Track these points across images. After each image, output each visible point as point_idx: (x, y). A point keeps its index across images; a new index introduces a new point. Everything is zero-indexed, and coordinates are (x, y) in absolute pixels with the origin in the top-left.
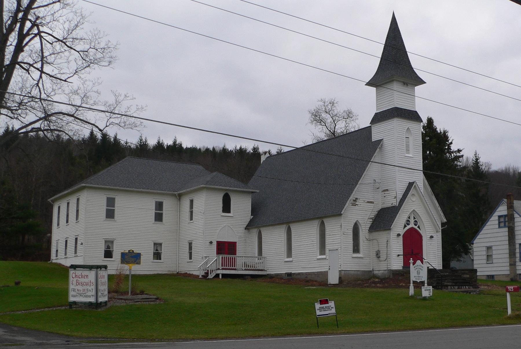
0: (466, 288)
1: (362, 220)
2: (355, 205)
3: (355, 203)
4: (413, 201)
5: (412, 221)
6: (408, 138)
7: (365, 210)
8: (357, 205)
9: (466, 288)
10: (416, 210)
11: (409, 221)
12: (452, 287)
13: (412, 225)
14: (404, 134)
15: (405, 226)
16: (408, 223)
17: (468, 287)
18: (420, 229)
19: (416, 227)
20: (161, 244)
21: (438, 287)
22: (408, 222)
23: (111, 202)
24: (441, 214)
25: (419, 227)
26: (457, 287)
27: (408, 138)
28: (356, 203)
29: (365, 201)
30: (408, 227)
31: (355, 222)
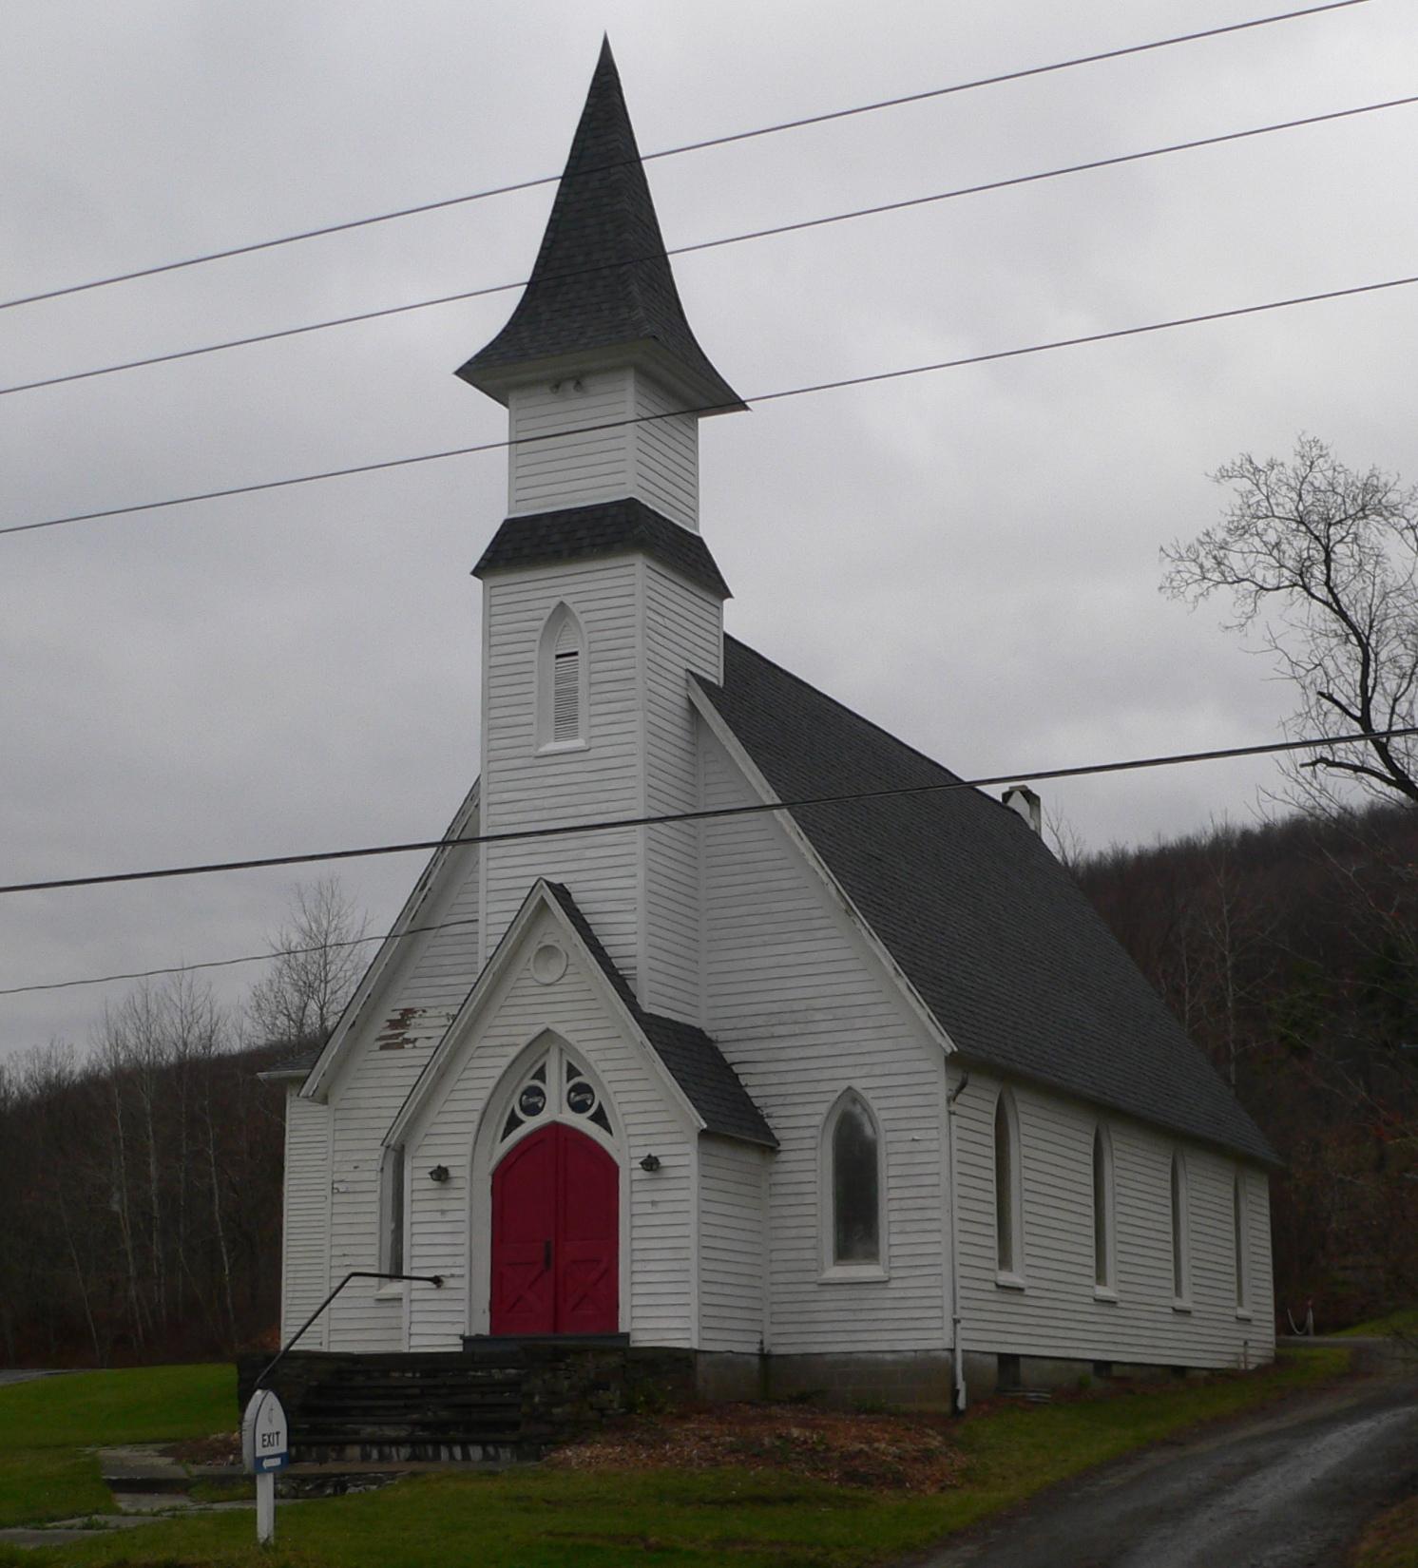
0: (466, 1456)
2: (400, 1046)
3: (403, 1034)
5: (556, 1088)
6: (575, 654)
8: (407, 1041)
9: (466, 1456)
10: (560, 1029)
11: (540, 1093)
12: (375, 1454)
13: (556, 1110)
15: (514, 1123)
16: (535, 1105)
17: (484, 1450)
18: (608, 1129)
19: (582, 1122)
22: (535, 1099)
25: (600, 1118)
26: (405, 1452)
27: (575, 654)
28: (406, 1036)
30: (531, 1124)
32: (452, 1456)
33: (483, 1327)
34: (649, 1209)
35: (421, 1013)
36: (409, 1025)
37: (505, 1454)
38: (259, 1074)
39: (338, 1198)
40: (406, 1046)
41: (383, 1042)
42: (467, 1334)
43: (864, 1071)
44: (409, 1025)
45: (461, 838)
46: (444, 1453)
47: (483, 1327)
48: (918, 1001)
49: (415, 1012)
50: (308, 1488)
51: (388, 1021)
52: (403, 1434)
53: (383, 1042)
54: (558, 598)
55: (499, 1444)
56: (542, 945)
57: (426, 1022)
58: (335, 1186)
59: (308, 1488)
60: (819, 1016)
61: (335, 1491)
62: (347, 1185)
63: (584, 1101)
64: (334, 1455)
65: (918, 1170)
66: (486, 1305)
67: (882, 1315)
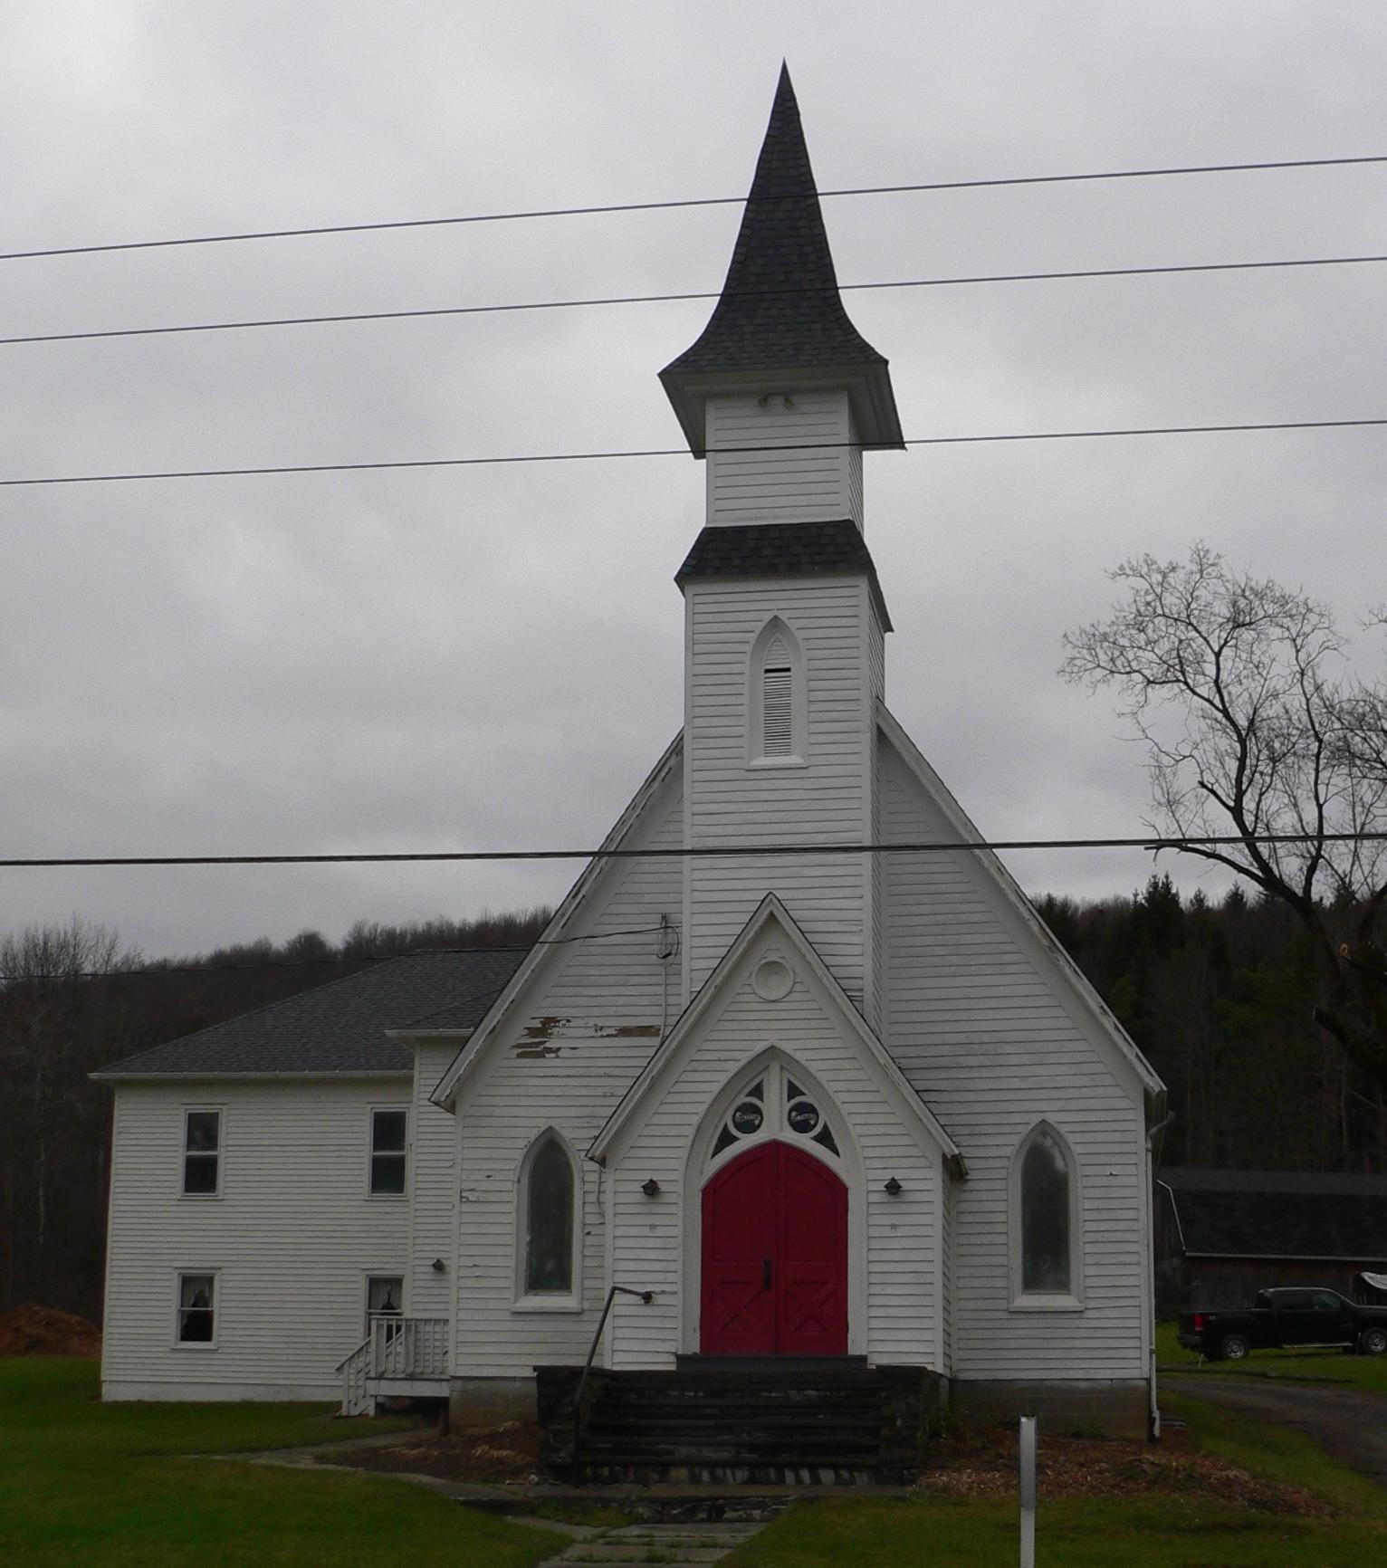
0: (816, 1480)
1: (577, 1123)
2: (541, 1055)
3: (545, 1042)
4: (774, 1001)
5: (775, 1107)
6: (788, 670)
7: (601, 1072)
8: (549, 1050)
9: (816, 1480)
10: (787, 1047)
11: (758, 1111)
12: (706, 1476)
13: (775, 1127)
14: (747, 658)
15: (726, 1139)
16: (752, 1122)
17: (837, 1475)
19: (805, 1142)
20: (396, 1282)
21: (589, 1471)
23: (203, 1131)
24: (1125, 1049)
25: (825, 1138)
26: (741, 1474)
27: (788, 670)
28: (547, 1045)
29: (601, 1029)
30: (746, 1142)
31: (533, 1134)
32: (799, 1481)
33: (694, 1347)
34: (887, 1232)
35: (564, 1022)
36: (550, 1034)
37: (862, 1478)
38: (89, 1074)
39: (466, 1208)
40: (547, 1055)
41: (520, 1050)
42: (679, 1353)
43: (1059, 1105)
44: (550, 1034)
45: (618, 850)
46: (789, 1476)
47: (694, 1347)
48: (1126, 1040)
49: (558, 1021)
50: (675, 1512)
51: (527, 1028)
52: (726, 1455)
53: (520, 1050)
54: (770, 612)
55: (851, 1468)
56: (763, 962)
57: (570, 1032)
58: (464, 1194)
59: (675, 1512)
60: (1008, 1049)
61: (710, 1514)
62: (478, 1194)
63: (806, 1121)
64: (656, 1476)
65: (1115, 1204)
66: (697, 1324)
67: (1078, 1344)
